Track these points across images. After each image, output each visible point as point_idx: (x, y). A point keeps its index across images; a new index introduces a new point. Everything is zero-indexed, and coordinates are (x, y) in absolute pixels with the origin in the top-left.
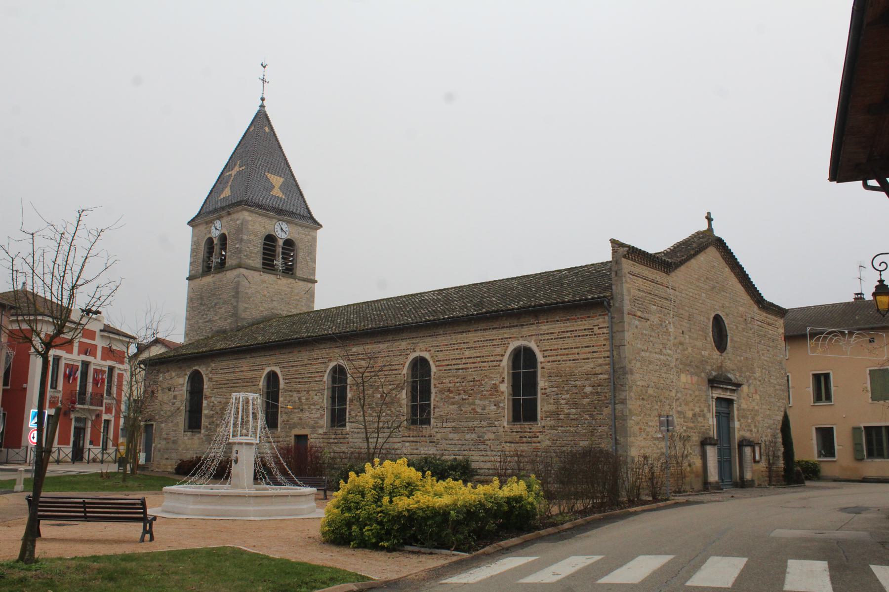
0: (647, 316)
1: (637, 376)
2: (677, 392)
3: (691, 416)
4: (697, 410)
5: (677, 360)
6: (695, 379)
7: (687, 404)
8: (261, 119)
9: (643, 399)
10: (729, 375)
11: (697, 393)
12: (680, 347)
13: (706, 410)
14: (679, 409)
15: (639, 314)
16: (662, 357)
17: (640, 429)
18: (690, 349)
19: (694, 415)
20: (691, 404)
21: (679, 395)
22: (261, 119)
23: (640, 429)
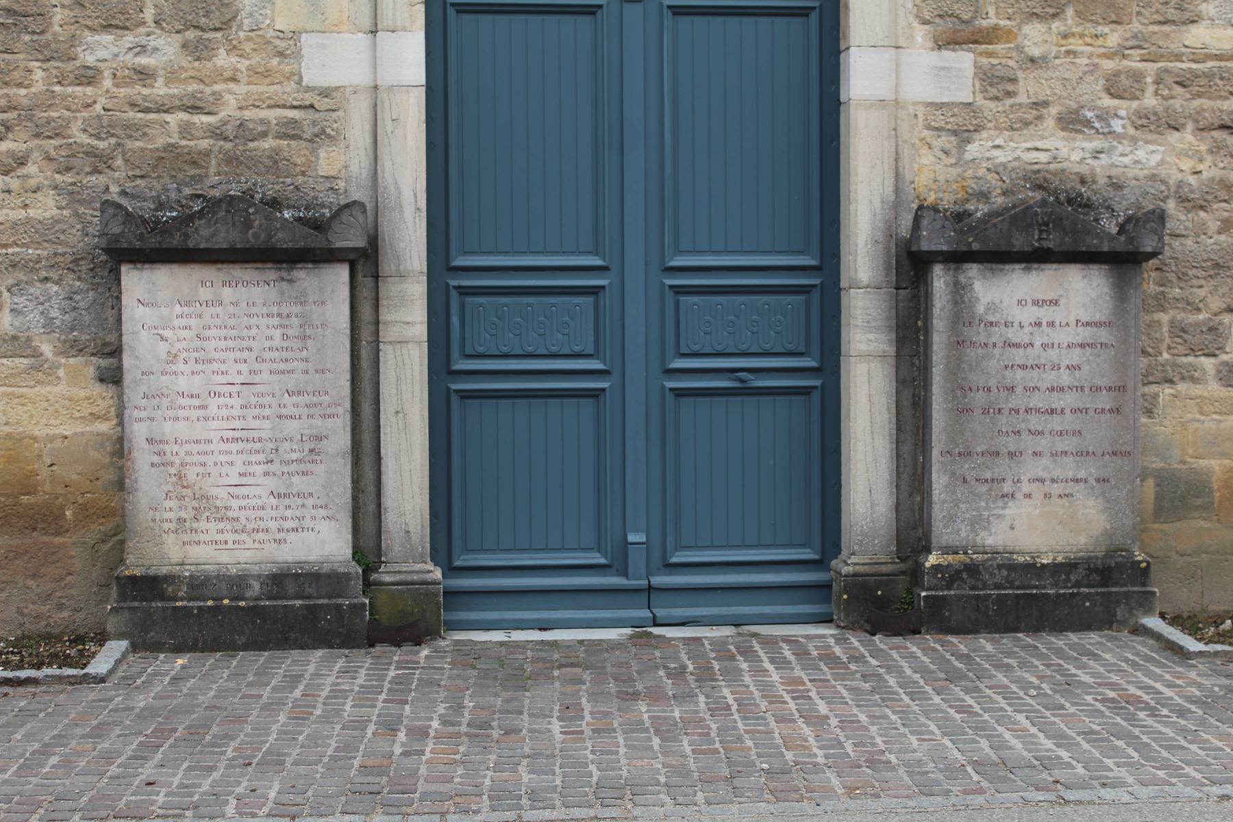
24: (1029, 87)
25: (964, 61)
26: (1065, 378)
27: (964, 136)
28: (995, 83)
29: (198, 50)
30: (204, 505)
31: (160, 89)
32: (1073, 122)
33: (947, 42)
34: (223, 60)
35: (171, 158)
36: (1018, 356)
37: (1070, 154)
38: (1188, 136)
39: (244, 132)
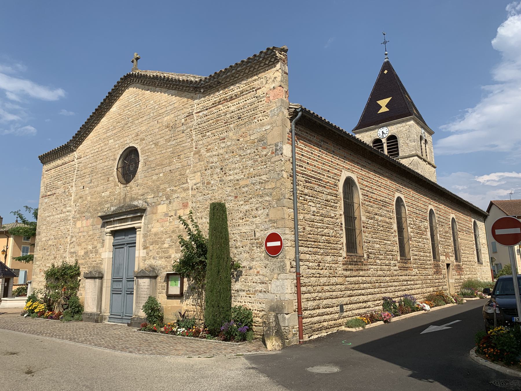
0: (53, 192)
1: (43, 235)
2: (72, 237)
3: (83, 253)
4: (90, 247)
5: (75, 212)
6: (90, 221)
7: (79, 245)
8: (387, 66)
9: (45, 249)
10: (135, 203)
11: (91, 233)
12: (80, 200)
13: (99, 245)
14: (72, 250)
15: (49, 193)
16: (62, 215)
17: (40, 269)
18: (89, 198)
19: (86, 253)
20: (83, 244)
21: (74, 239)
22: (387, 66)
23: (40, 269)
24: (150, 254)
25: (145, 251)
26: (145, 293)
27: (145, 260)
28: (147, 253)
29: (96, 255)
30: (89, 306)
31: (94, 259)
32: (154, 258)
33: (144, 249)
34: (97, 256)
35: (94, 267)
36: (142, 290)
37: (153, 262)
38: (163, 260)
39: (97, 264)
